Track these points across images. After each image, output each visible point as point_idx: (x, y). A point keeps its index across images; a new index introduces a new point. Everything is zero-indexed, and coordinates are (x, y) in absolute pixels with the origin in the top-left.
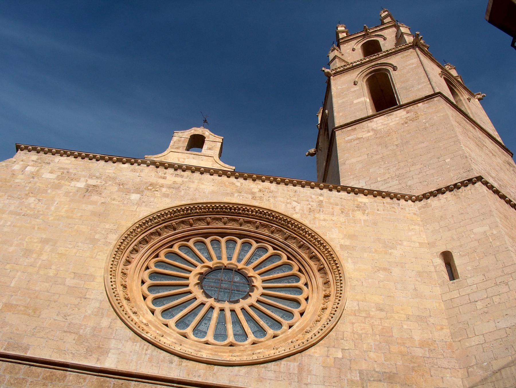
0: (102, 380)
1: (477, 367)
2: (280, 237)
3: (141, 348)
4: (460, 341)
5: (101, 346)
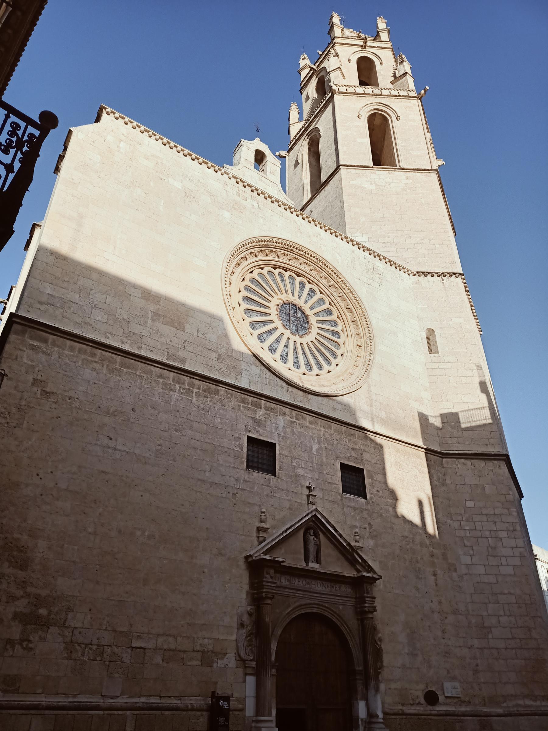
0: (243, 397)
2: (326, 283)
4: (437, 402)
5: (235, 366)
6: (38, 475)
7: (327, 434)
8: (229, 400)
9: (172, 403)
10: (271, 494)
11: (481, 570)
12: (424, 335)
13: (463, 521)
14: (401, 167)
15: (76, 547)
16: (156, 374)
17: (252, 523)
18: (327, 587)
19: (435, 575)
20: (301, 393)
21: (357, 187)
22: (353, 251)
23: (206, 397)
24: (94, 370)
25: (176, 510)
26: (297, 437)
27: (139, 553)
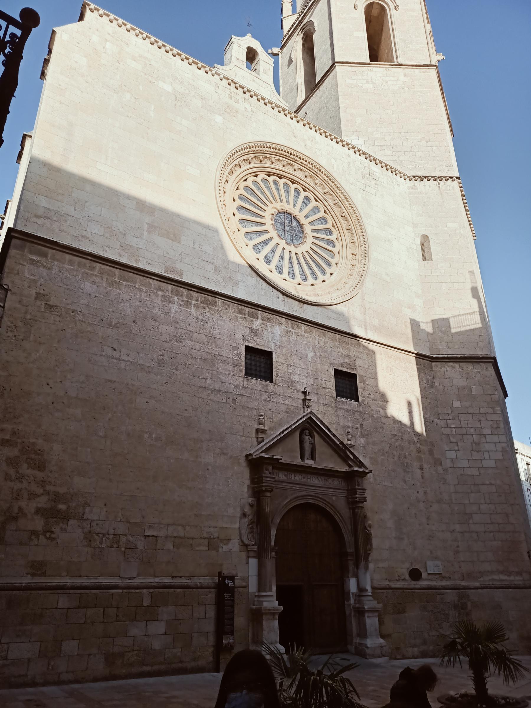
0: (240, 307)
1: (438, 329)
2: (321, 190)
3: (258, 283)
4: (428, 308)
5: (232, 278)
6: (48, 384)
7: (322, 342)
8: (226, 311)
9: (172, 315)
10: (268, 399)
11: (465, 463)
12: (418, 242)
13: (449, 420)
14: (399, 63)
15: (89, 450)
16: (155, 287)
17: (252, 426)
18: (321, 481)
19: (421, 468)
20: (297, 303)
21: (353, 86)
22: (349, 156)
23: (204, 308)
24: (94, 283)
25: (181, 415)
26: (292, 345)
27: (148, 454)
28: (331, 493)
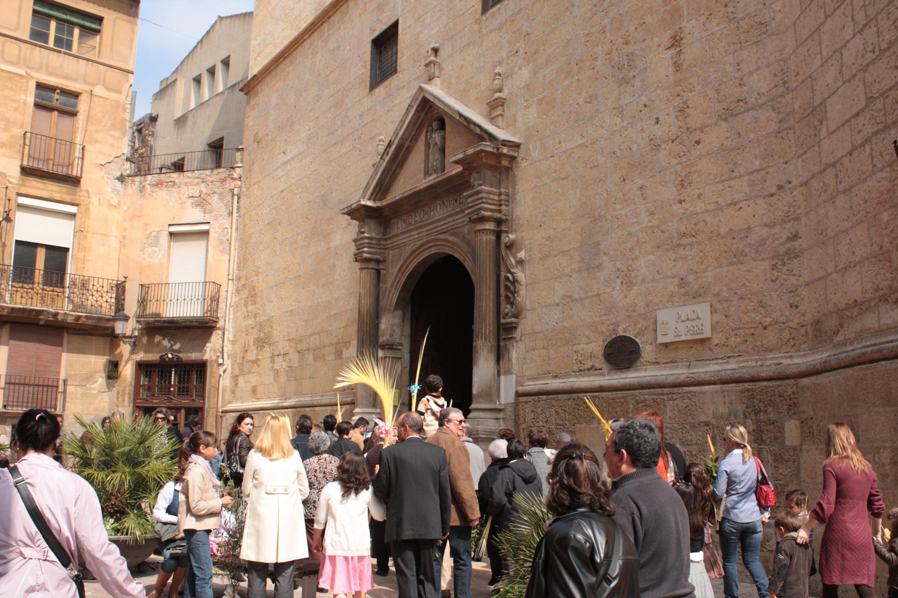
28: (461, 223)
